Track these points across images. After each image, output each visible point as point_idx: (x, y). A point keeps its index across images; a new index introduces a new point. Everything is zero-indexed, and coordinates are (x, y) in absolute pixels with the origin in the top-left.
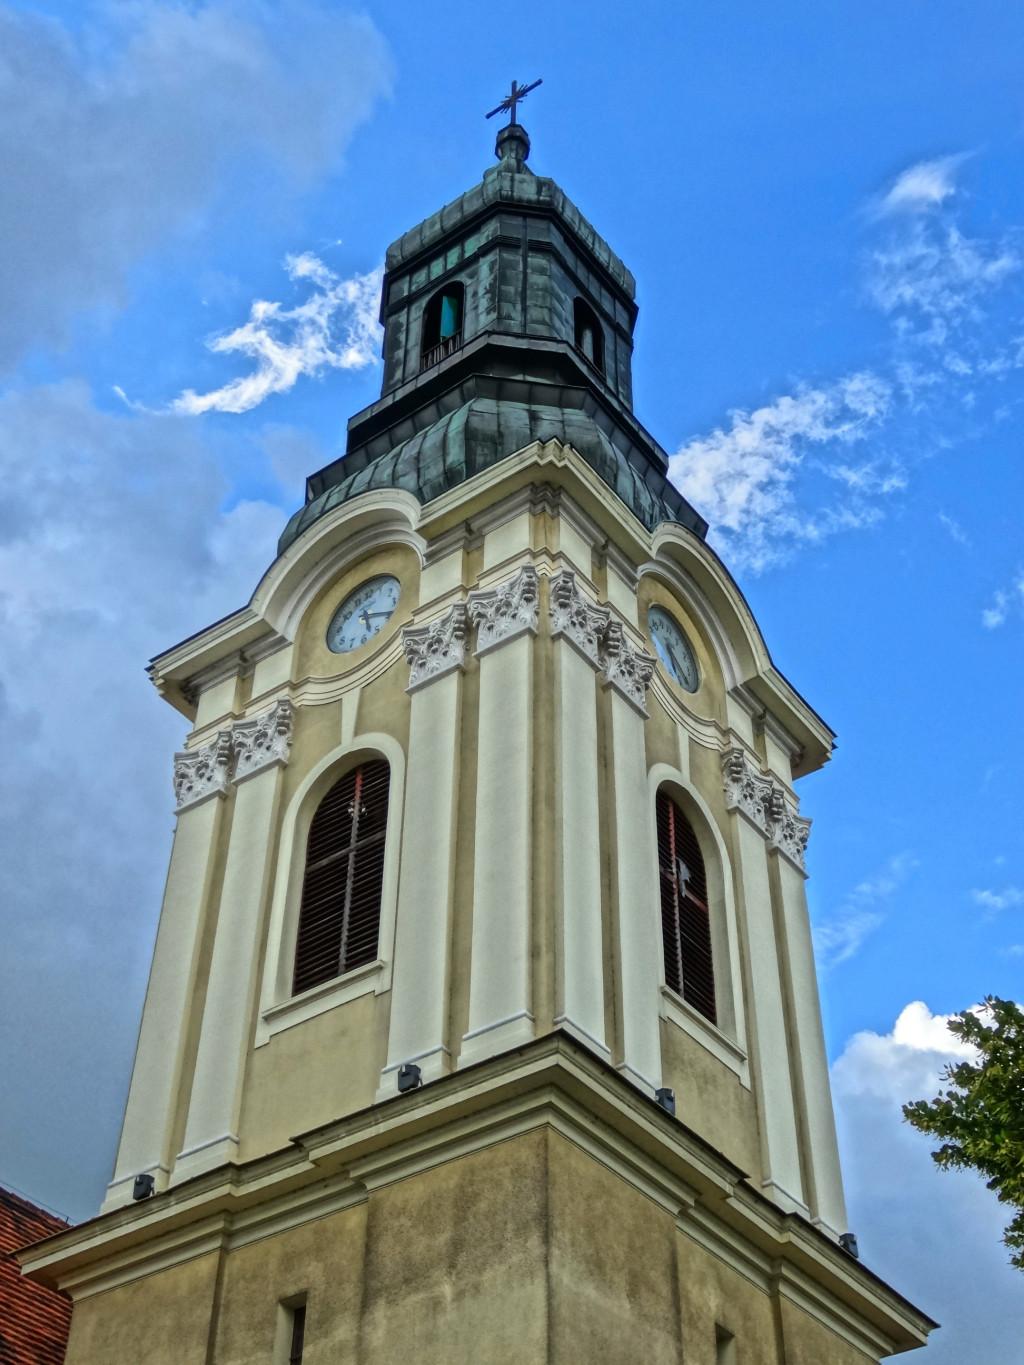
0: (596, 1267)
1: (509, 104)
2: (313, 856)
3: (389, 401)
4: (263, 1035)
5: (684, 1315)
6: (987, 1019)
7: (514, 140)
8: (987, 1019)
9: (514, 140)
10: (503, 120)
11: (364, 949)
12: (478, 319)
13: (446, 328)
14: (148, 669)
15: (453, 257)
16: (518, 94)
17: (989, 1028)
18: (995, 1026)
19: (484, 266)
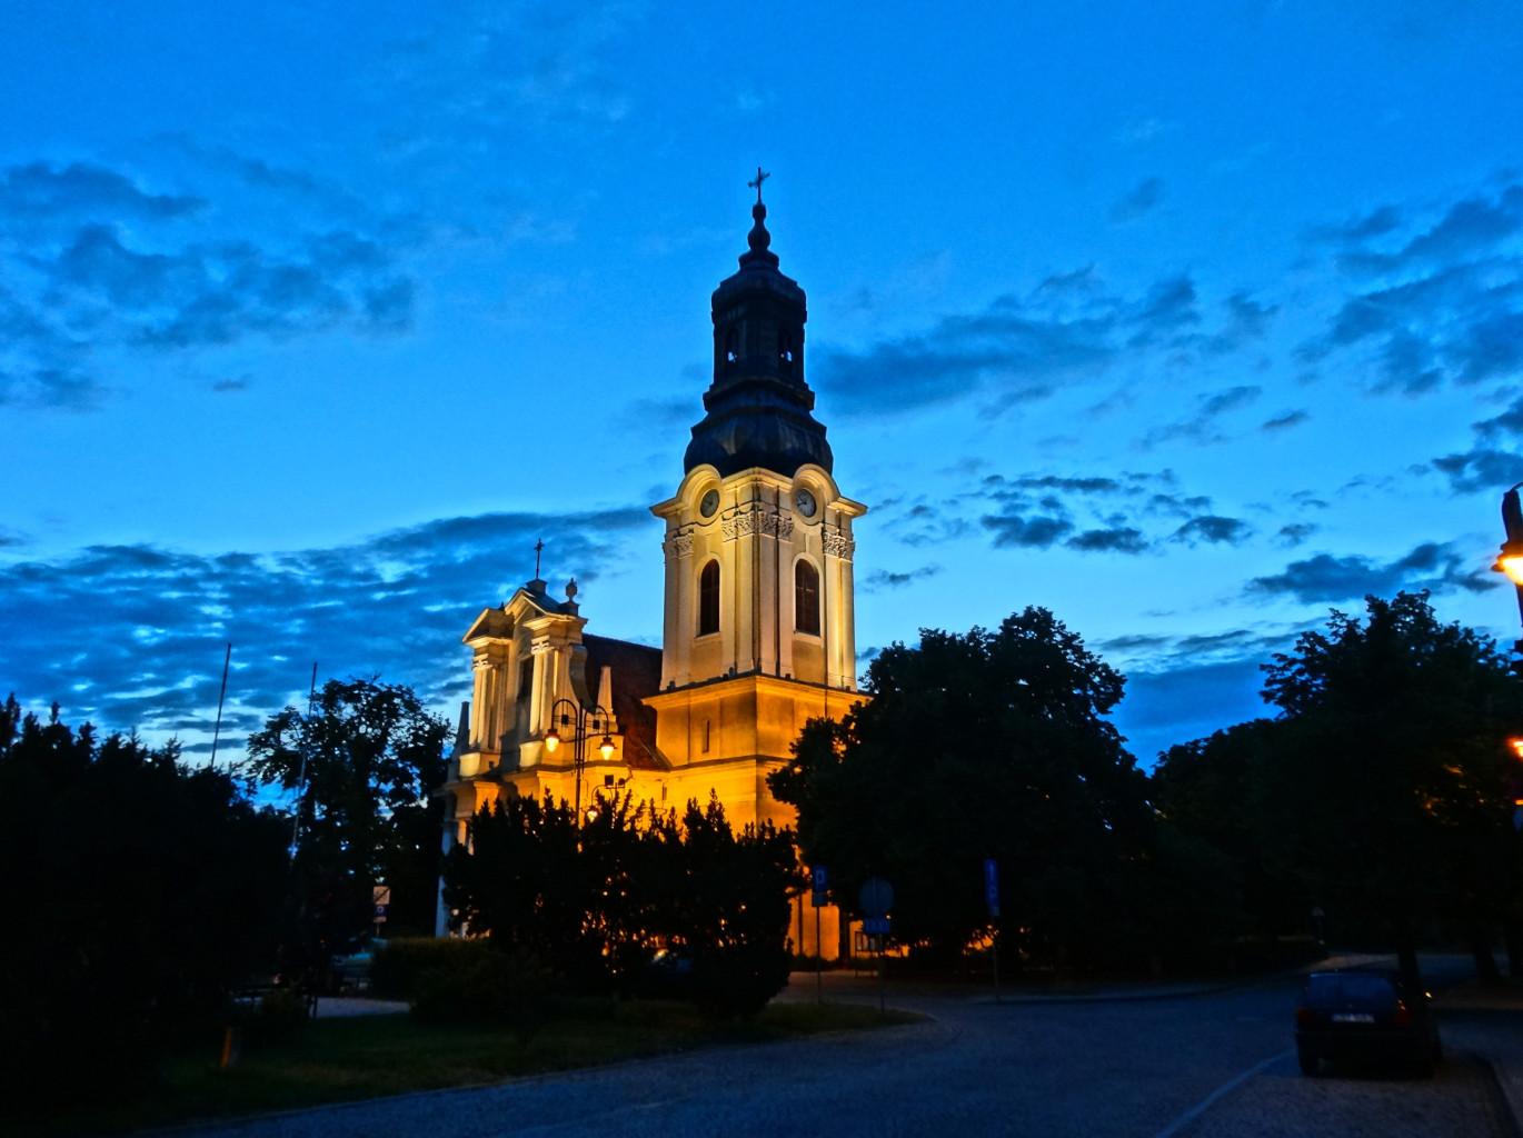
9: (759, 212)
19: (745, 323)
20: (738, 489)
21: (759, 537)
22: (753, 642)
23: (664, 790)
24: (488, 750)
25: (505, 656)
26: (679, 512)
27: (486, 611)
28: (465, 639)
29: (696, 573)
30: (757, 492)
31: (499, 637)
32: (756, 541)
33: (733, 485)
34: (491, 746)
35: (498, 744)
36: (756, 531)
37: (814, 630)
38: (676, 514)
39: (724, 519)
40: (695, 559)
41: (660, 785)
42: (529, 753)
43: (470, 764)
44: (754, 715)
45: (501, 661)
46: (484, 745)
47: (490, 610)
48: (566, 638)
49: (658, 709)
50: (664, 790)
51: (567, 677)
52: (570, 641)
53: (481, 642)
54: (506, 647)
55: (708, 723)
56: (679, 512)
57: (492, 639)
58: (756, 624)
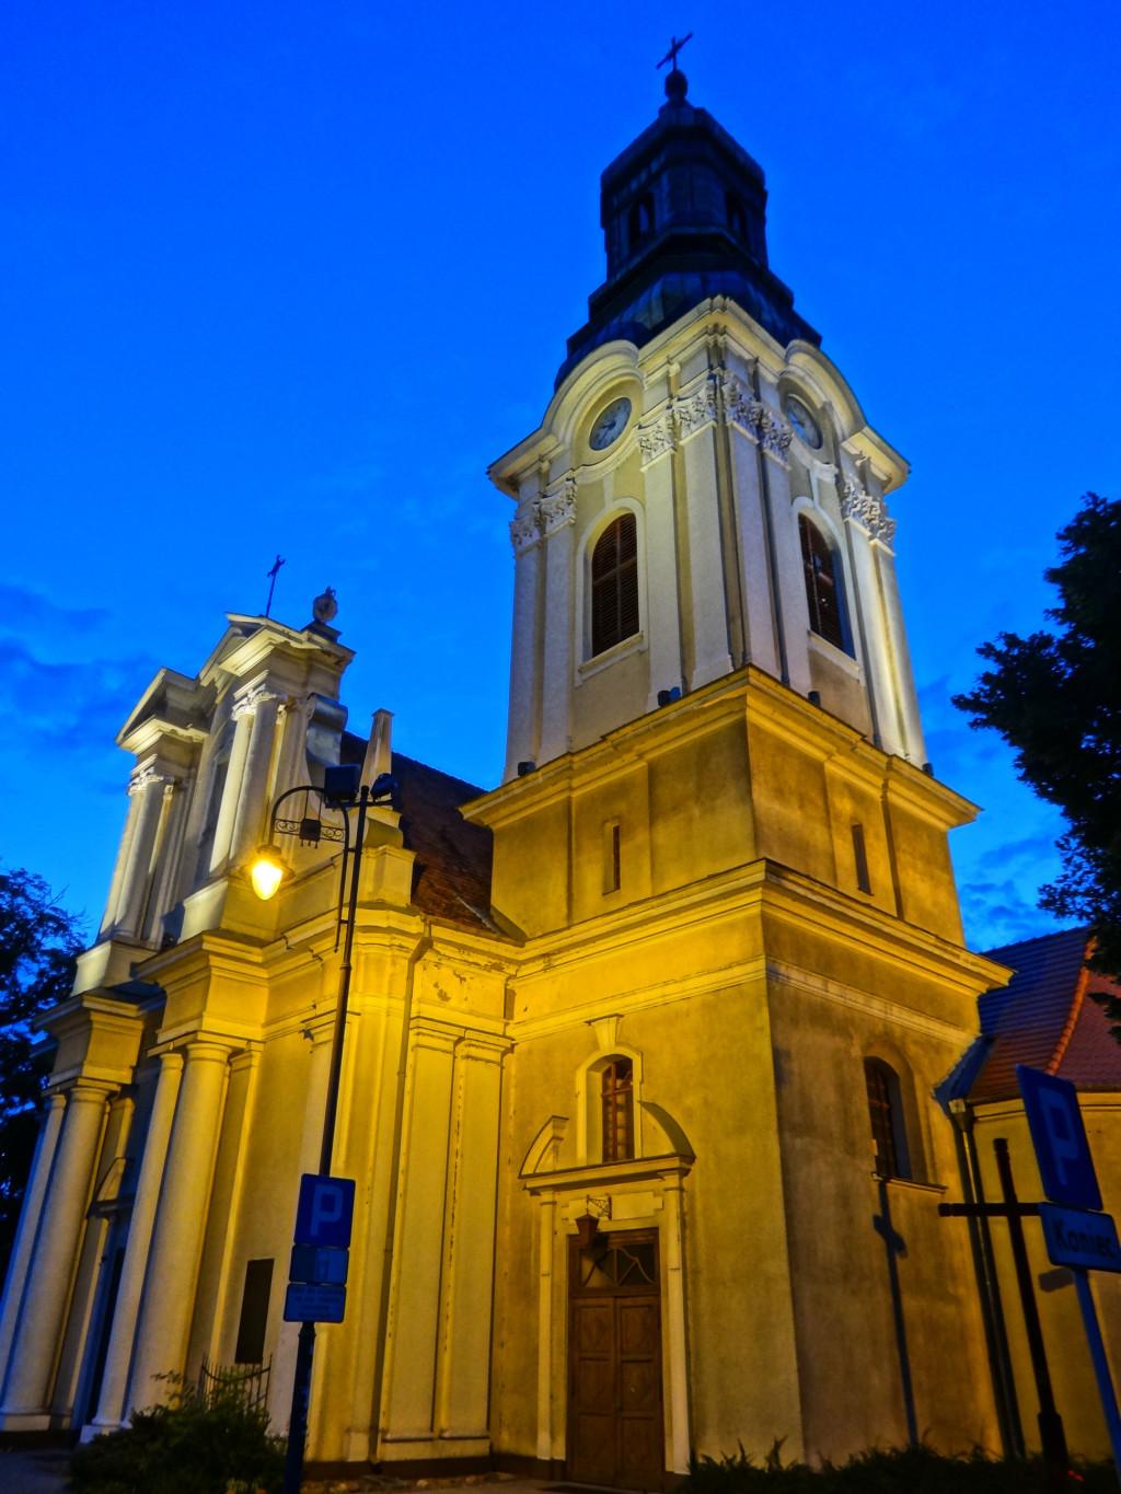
0: (779, 793)
1: (672, 55)
2: (595, 577)
3: (614, 281)
4: (578, 680)
5: (832, 815)
6: (1000, 646)
7: (676, 84)
8: (1000, 646)
9: (676, 84)
10: (667, 69)
11: (630, 625)
12: (664, 215)
13: (644, 227)
14: (488, 473)
15: (644, 176)
16: (676, 47)
17: (1000, 651)
18: (1004, 649)
19: (664, 179)
20: (675, 368)
21: (726, 430)
22: (729, 620)
23: (509, 997)
25: (193, 765)
26: (545, 466)
27: (161, 674)
28: (121, 736)
29: (581, 550)
30: (717, 356)
32: (722, 434)
33: (661, 360)
34: (145, 937)
36: (721, 418)
37: (844, 644)
38: (539, 472)
39: (640, 427)
40: (576, 528)
41: (495, 983)
42: (200, 908)
43: (92, 968)
44: (745, 773)
45: (182, 773)
46: (130, 926)
47: (169, 671)
48: (305, 684)
49: (494, 828)
50: (509, 997)
51: (301, 749)
52: (310, 690)
53: (146, 736)
54: (195, 749)
55: (617, 831)
56: (545, 466)
57: (168, 727)
58: (734, 592)
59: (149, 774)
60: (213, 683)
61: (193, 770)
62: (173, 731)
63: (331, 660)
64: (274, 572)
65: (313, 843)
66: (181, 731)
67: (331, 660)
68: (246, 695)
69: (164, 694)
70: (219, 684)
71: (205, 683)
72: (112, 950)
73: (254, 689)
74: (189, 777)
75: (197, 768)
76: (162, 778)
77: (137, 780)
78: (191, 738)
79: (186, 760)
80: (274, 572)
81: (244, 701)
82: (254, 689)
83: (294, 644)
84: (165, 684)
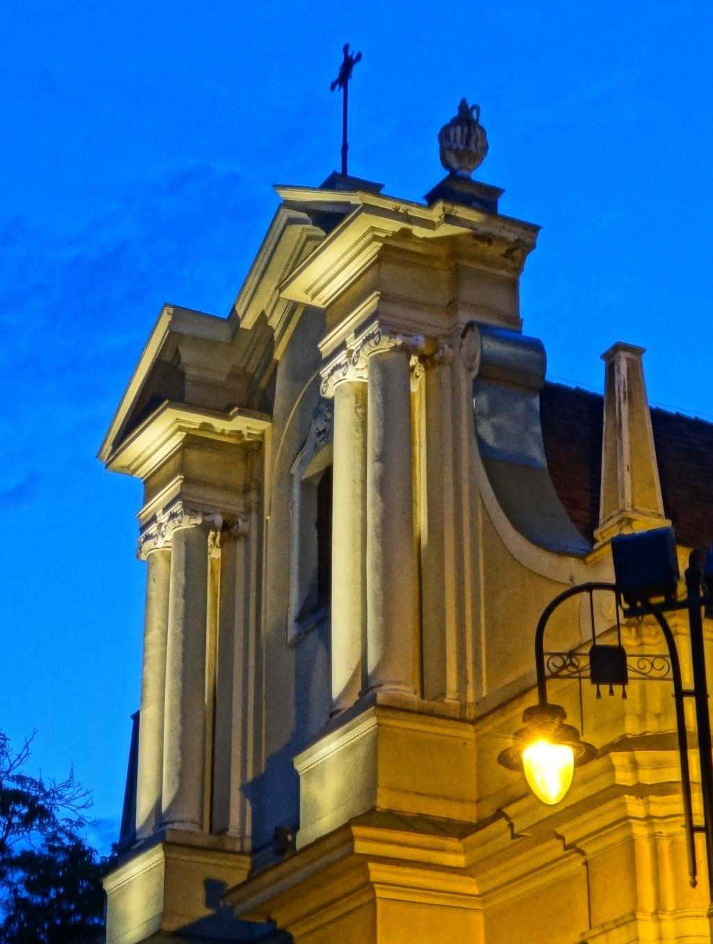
24: (204, 838)
25: (253, 485)
27: (166, 319)
28: (108, 447)
31: (223, 412)
34: (218, 828)
35: (239, 816)
42: (328, 775)
45: (235, 504)
46: (189, 812)
47: (179, 312)
48: (452, 307)
51: (468, 448)
52: (465, 317)
53: (157, 441)
54: (252, 450)
57: (195, 420)
59: (173, 516)
60: (263, 319)
61: (253, 496)
62: (205, 427)
63: (496, 250)
64: (344, 78)
65: (618, 689)
66: (219, 424)
67: (496, 250)
68: (343, 346)
69: (177, 354)
70: (275, 321)
71: (248, 323)
72: (167, 858)
73: (358, 331)
74: (248, 511)
75: (260, 490)
76: (199, 521)
77: (152, 529)
78: (239, 434)
79: (237, 477)
80: (344, 78)
81: (341, 358)
82: (358, 331)
83: (419, 232)
84: (173, 338)
